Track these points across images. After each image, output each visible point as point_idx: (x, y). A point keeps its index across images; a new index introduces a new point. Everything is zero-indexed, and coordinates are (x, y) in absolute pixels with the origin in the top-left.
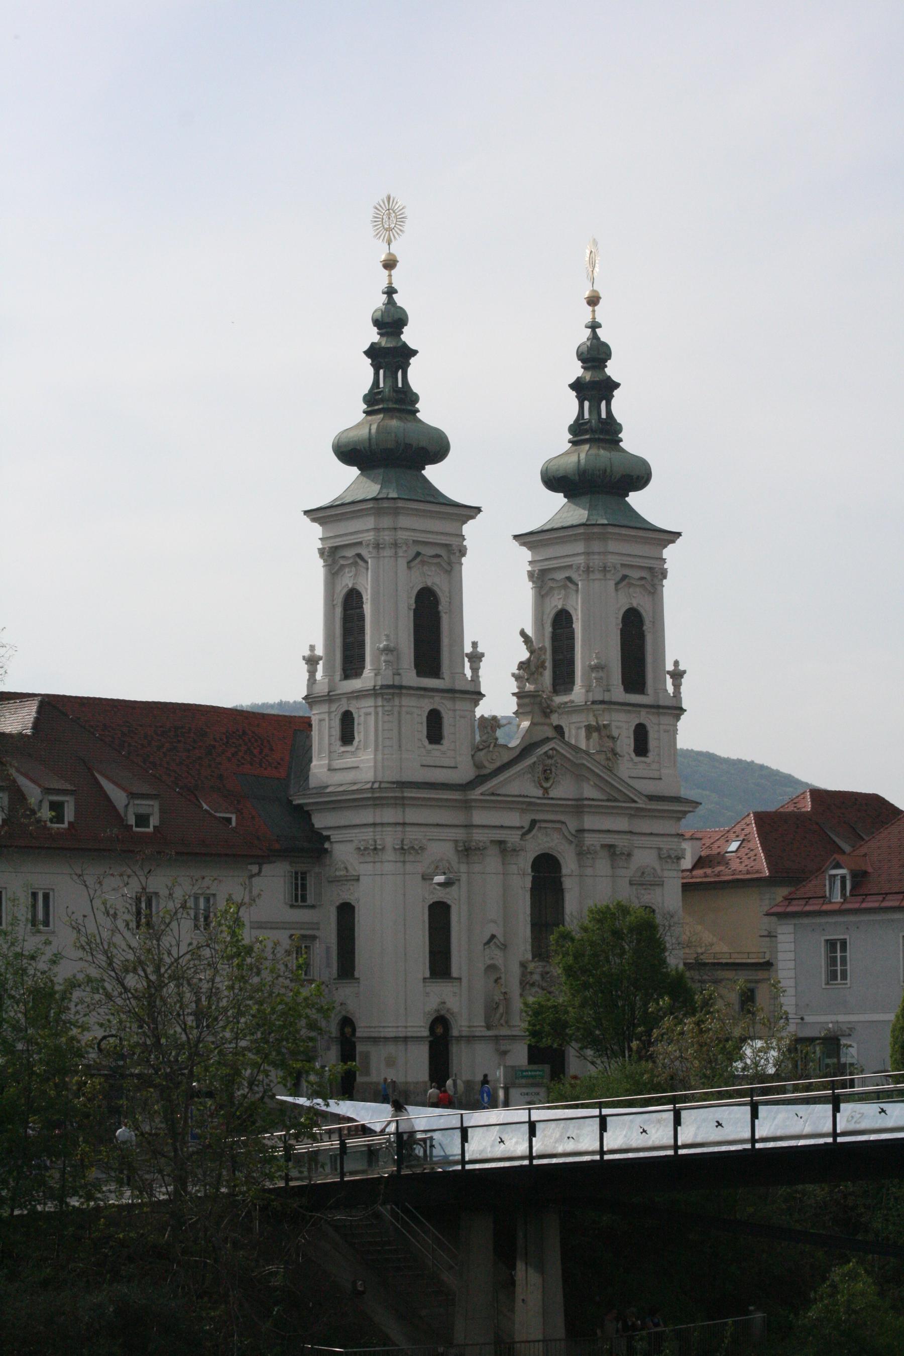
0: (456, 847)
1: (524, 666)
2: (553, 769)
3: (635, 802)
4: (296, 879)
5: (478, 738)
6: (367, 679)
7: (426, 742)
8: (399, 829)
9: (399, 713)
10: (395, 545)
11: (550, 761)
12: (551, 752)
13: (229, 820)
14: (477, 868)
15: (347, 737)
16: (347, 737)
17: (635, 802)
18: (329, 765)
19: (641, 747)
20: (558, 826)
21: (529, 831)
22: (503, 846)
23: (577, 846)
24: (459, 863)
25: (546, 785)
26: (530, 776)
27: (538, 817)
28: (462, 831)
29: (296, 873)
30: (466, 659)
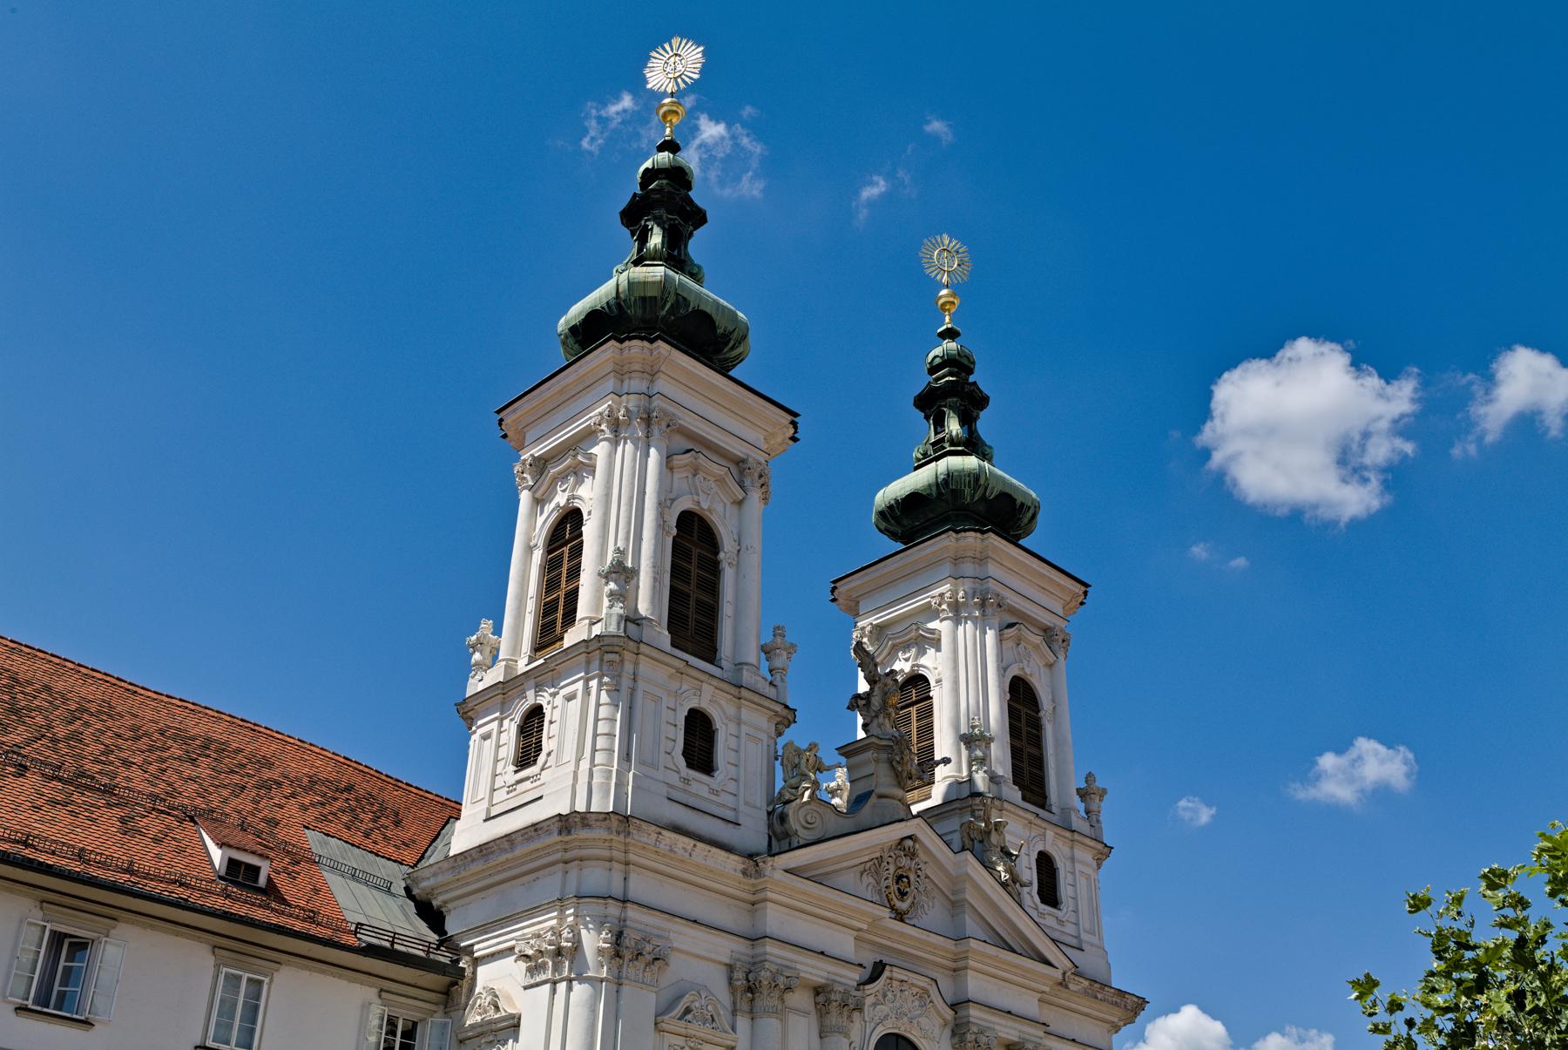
0: (730, 980)
1: (861, 702)
2: (912, 877)
3: (1050, 964)
4: (392, 1032)
5: (779, 784)
6: (572, 637)
7: (682, 762)
8: (614, 909)
9: (633, 690)
10: (648, 421)
11: (904, 861)
12: (909, 843)
13: (257, 870)
14: (770, 1025)
15: (527, 755)
16: (527, 755)
17: (1050, 964)
18: (488, 810)
19: (1049, 895)
20: (922, 982)
21: (873, 978)
22: (821, 999)
23: (954, 1034)
24: (734, 1012)
25: (902, 906)
26: (871, 880)
27: (886, 960)
28: (741, 947)
29: (392, 1023)
30: (763, 656)
